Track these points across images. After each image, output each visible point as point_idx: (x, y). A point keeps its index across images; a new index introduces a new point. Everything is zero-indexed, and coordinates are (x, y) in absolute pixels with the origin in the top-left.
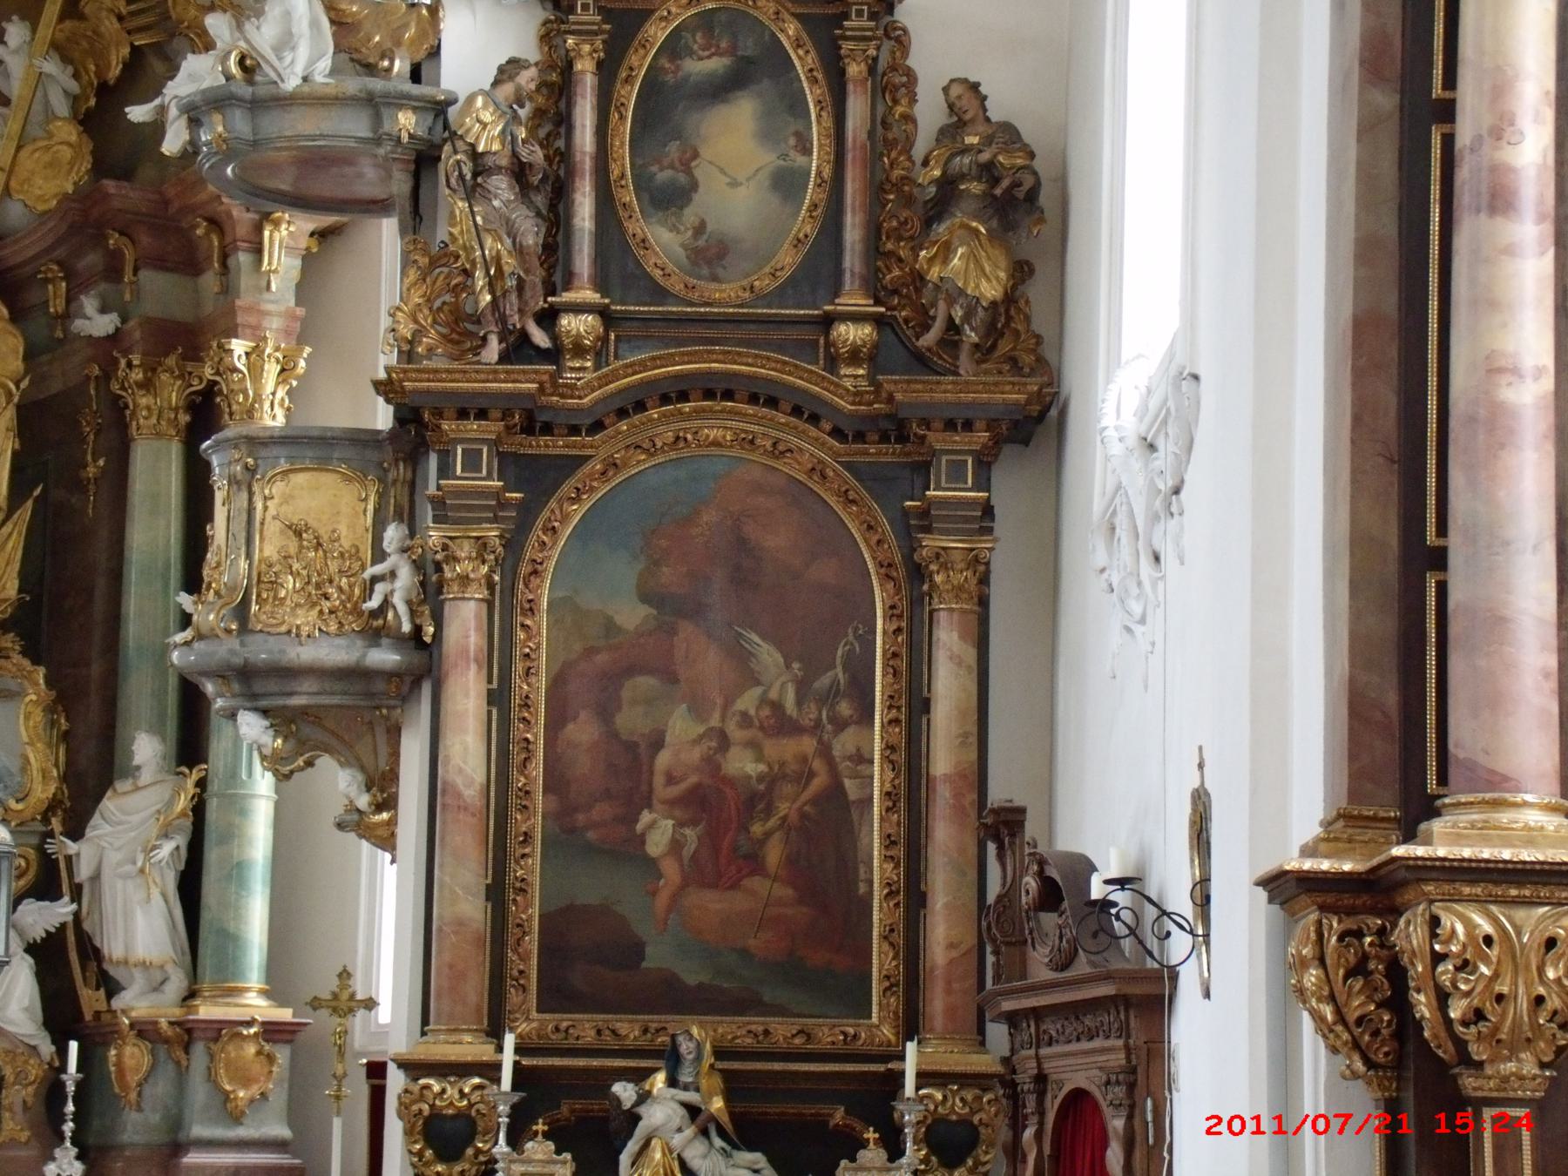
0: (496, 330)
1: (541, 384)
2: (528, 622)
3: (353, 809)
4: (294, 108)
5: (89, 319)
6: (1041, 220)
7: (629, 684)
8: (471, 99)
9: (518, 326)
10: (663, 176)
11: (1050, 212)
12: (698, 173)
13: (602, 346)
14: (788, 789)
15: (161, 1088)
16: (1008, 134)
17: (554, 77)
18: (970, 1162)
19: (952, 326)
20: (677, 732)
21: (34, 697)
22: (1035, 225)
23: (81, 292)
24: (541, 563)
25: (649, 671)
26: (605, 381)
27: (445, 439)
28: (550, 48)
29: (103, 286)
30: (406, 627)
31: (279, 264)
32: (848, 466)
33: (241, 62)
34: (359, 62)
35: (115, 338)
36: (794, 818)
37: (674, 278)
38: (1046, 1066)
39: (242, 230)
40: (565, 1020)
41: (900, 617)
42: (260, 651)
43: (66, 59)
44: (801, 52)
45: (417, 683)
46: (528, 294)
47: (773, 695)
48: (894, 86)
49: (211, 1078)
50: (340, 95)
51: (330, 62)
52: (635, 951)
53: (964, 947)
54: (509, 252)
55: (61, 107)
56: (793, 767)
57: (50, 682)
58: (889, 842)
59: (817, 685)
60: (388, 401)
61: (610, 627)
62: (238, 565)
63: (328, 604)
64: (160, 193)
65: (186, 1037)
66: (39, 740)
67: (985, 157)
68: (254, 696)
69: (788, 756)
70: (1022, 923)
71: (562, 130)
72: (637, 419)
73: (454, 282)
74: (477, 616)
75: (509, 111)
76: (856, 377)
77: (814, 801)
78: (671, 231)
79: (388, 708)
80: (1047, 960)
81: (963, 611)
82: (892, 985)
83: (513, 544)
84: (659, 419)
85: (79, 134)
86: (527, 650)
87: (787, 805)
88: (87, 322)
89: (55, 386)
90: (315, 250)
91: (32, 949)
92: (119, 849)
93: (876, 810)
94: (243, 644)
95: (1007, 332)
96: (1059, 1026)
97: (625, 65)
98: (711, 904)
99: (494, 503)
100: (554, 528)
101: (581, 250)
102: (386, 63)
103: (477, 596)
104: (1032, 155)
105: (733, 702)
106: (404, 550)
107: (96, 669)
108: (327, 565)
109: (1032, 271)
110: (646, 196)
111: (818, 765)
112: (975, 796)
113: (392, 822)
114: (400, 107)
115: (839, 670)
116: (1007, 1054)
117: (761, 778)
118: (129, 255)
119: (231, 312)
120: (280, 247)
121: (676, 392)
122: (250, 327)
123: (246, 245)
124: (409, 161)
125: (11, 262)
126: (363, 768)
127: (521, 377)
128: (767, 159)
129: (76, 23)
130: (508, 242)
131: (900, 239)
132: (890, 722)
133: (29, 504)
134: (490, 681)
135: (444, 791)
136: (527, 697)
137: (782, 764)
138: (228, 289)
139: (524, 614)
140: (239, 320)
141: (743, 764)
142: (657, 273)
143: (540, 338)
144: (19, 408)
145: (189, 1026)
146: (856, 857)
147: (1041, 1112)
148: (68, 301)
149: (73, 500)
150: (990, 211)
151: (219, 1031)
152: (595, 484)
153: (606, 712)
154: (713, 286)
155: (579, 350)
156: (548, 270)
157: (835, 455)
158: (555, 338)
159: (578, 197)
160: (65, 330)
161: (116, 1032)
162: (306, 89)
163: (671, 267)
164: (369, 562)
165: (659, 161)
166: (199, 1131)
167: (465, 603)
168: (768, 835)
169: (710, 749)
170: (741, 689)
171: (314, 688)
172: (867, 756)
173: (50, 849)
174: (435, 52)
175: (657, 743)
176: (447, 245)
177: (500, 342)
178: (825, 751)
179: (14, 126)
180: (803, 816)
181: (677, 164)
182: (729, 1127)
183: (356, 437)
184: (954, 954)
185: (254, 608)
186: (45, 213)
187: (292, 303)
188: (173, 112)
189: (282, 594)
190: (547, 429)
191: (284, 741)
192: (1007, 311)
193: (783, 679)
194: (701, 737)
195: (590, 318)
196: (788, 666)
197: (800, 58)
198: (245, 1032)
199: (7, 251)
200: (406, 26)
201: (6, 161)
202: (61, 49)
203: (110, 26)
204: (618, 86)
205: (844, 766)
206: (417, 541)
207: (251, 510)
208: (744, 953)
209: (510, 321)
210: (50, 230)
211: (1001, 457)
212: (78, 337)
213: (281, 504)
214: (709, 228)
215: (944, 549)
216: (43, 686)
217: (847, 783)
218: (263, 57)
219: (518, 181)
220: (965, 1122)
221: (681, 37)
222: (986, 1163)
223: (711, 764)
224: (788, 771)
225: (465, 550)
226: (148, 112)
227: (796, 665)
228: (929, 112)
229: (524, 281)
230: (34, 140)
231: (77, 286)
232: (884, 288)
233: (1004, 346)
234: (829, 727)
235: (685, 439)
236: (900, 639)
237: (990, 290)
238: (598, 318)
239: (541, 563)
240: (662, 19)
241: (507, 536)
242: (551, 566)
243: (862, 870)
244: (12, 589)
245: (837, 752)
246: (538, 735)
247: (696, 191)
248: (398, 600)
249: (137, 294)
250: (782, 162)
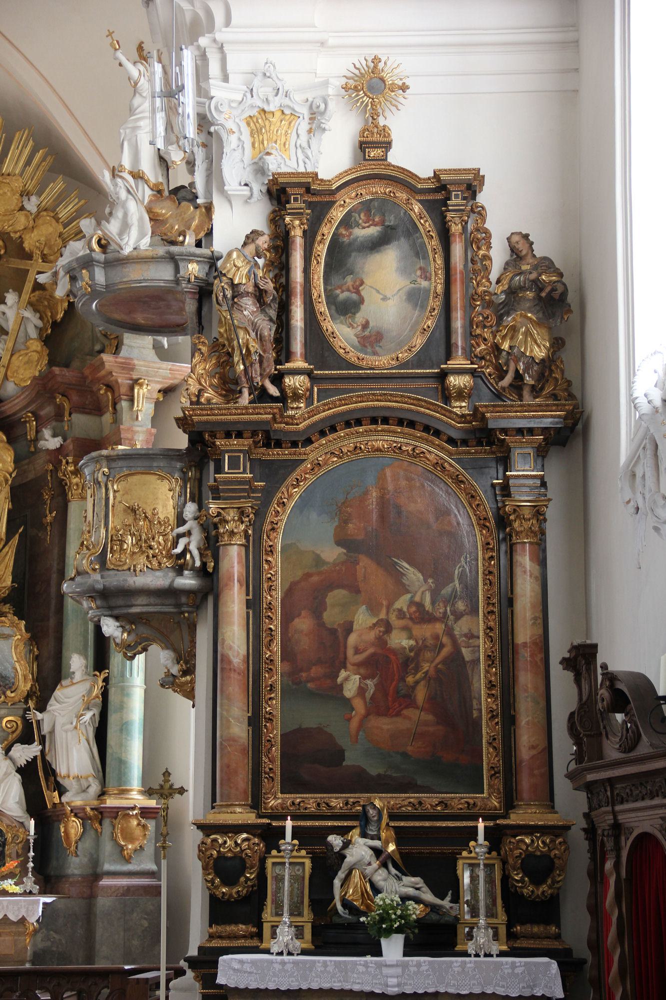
0: (247, 386)
1: (274, 414)
2: (270, 559)
3: (169, 674)
4: (128, 265)
5: (47, 440)
6: (570, 311)
7: (330, 595)
8: (230, 254)
9: (260, 384)
10: (343, 296)
11: (574, 307)
12: (363, 293)
13: (310, 394)
14: (428, 655)
15: (87, 844)
16: (546, 264)
17: (279, 243)
18: (549, 881)
19: (518, 376)
20: (360, 622)
21: (19, 637)
22: (566, 314)
23: (43, 427)
24: (277, 524)
25: (340, 586)
26: (311, 414)
27: (218, 452)
28: (276, 226)
29: (54, 423)
30: (198, 564)
31: (142, 406)
32: (458, 461)
33: (99, 242)
34: (166, 240)
35: (59, 450)
36: (432, 672)
37: (351, 354)
38: (620, 817)
39: (123, 390)
40: (298, 798)
41: (492, 550)
42: (114, 580)
43: (36, 310)
44: (422, 221)
45: (205, 598)
46: (265, 364)
47: (417, 599)
48: (478, 239)
49: (114, 840)
50: (155, 256)
51: (149, 239)
52: (340, 754)
53: (541, 747)
54: (254, 340)
55: (33, 334)
56: (430, 642)
57: (27, 629)
58: (491, 685)
59: (443, 592)
60: (185, 432)
61: (318, 560)
62: (100, 531)
63: (152, 551)
64: (83, 373)
65: (100, 816)
66: (22, 660)
67: (533, 276)
68: (110, 608)
69: (428, 634)
70: (598, 722)
71: (284, 272)
72: (331, 437)
73: (222, 360)
74: (239, 554)
75: (252, 260)
76: (461, 407)
77: (444, 661)
78: (349, 327)
79: (188, 612)
80: (618, 746)
81: (530, 543)
82: (496, 773)
83: (260, 513)
84: (344, 436)
85: (42, 347)
86: (269, 575)
87: (428, 664)
88: (46, 442)
89: (31, 476)
90: (161, 399)
91: (19, 770)
92: (63, 716)
93: (482, 666)
94: (102, 577)
95: (550, 379)
96: (628, 790)
97: (320, 233)
98: (384, 725)
99: (247, 487)
100: (284, 502)
101: (296, 339)
102: (181, 238)
103: (238, 543)
104: (561, 275)
105: (393, 603)
106: (196, 519)
107: (52, 622)
108: (151, 529)
109: (563, 343)
110: (333, 307)
111: (445, 640)
112: (543, 656)
113: (193, 682)
114: (190, 261)
115: (457, 582)
116: (587, 811)
117: (411, 649)
118: (67, 406)
119: (118, 431)
120: (143, 398)
121: (353, 421)
122: (128, 439)
123: (125, 397)
124: (195, 293)
125: (9, 413)
126: (175, 650)
127: (262, 411)
129: (41, 292)
130: (253, 334)
131: (485, 327)
132: (489, 613)
133: (17, 536)
134: (248, 595)
135: (222, 660)
136: (270, 603)
137: (424, 640)
138: (117, 421)
139: (267, 554)
140: (122, 436)
141: (400, 641)
142: (342, 351)
143: (273, 391)
144: (12, 489)
145: (102, 810)
146: (471, 696)
147: (618, 849)
148: (37, 432)
149: (40, 535)
150: (538, 308)
151: (116, 813)
152: (307, 476)
153: (318, 610)
154: (375, 358)
155: (296, 397)
156: (277, 353)
157: (450, 454)
158: (282, 390)
159: (293, 308)
160: (35, 447)
161: (64, 814)
162: (135, 253)
163: (349, 348)
164: (176, 526)
165: (340, 287)
166: (107, 867)
167: (232, 546)
168: (417, 683)
169: (380, 631)
170: (397, 597)
171: (144, 602)
172: (476, 634)
173: (28, 717)
174: (210, 234)
175: (348, 628)
176: (217, 340)
177: (250, 395)
178: (449, 632)
179: (10, 345)
180: (437, 670)
181: (351, 288)
182: (399, 862)
183: (166, 453)
184: (534, 752)
185: (109, 555)
186: (25, 387)
187: (150, 426)
188: (61, 273)
189: (125, 547)
190: (279, 444)
191: (128, 635)
192: (550, 366)
193: (422, 589)
194: (374, 625)
195: (302, 378)
196: (425, 581)
197: (422, 224)
198: (131, 813)
199: (6, 407)
200: (193, 219)
201: (5, 361)
202: (34, 306)
204: (316, 245)
205: (461, 640)
206: (203, 512)
207: (107, 499)
208: (405, 755)
209: (255, 380)
210: (27, 395)
211: (549, 452)
212: (41, 450)
213: (124, 495)
214: (371, 324)
215: (519, 506)
216: (24, 631)
217: (464, 650)
218: (111, 238)
219: (259, 301)
220: (545, 856)
221: (352, 216)
222: (559, 882)
223: (381, 642)
224: (428, 644)
225: (231, 515)
226: (48, 277)
227: (430, 581)
228: (498, 255)
229: (263, 357)
230: (20, 351)
231: (41, 423)
232: (476, 356)
233: (548, 389)
234: (452, 617)
235: (361, 448)
236: (493, 562)
237: (540, 353)
238: (307, 377)
239: (277, 524)
240: (341, 206)
241: (257, 508)
242: (282, 525)
243: (475, 702)
244: (8, 582)
245: (456, 633)
246: (276, 625)
247: (363, 304)
248: (193, 547)
249: (71, 427)
250: (413, 285)
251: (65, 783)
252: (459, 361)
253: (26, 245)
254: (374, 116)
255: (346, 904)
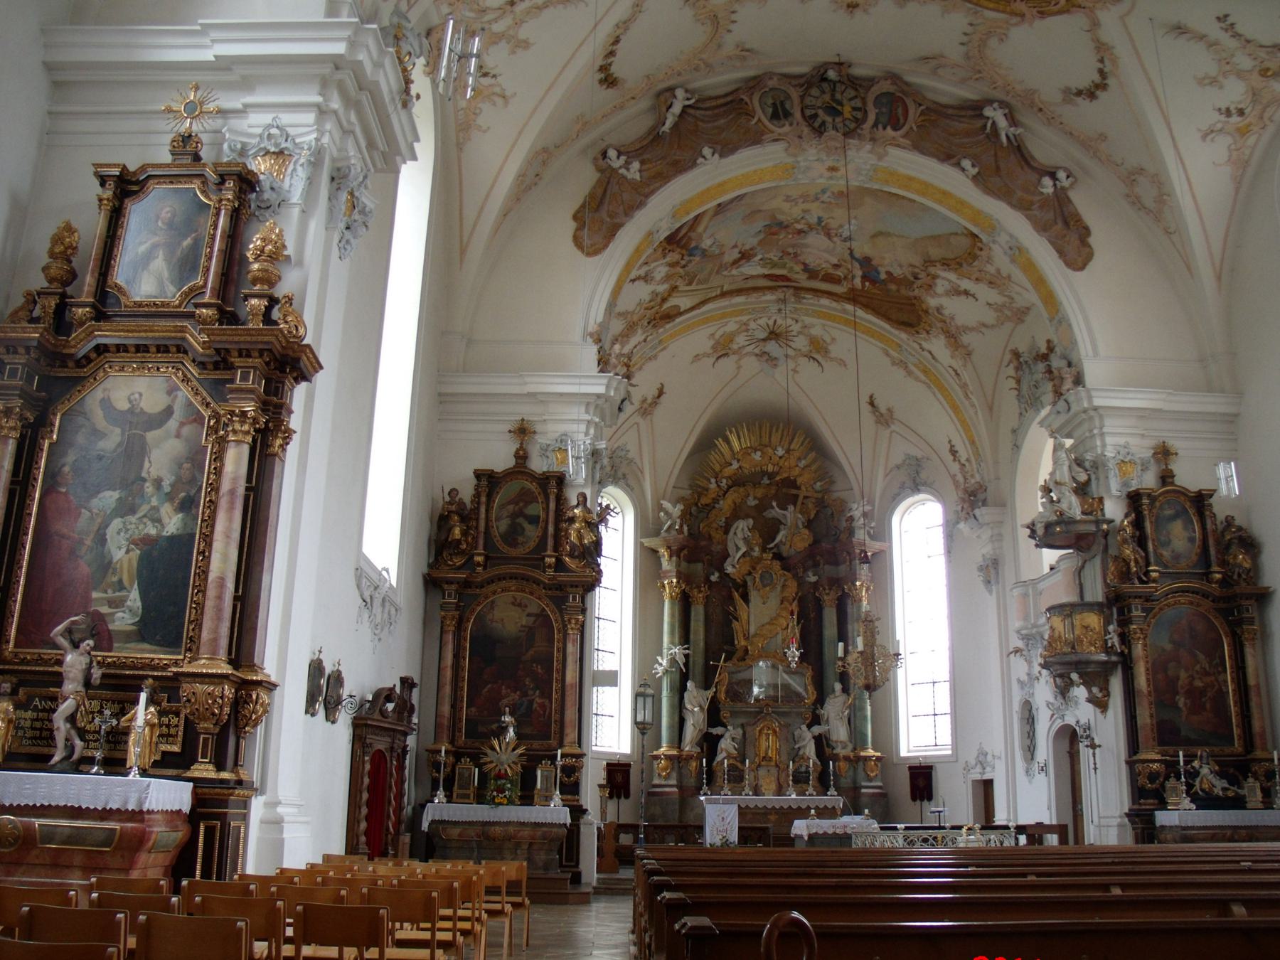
15: (851, 773)
16: (1240, 529)
19: (1239, 575)
40: (1166, 748)
49: (864, 770)
55: (801, 526)
91: (814, 737)
119: (855, 574)
128: (1186, 534)
141: (1198, 683)
143: (1144, 579)
155: (1154, 581)
175: (1178, 678)
178: (1217, 680)
202: (801, 513)
203: (810, 506)
223: (1191, 684)
225: (1138, 631)
231: (805, 570)
251: (834, 745)
252: (1215, 568)
253: (798, 483)
254: (1166, 465)
255: (1202, 790)
